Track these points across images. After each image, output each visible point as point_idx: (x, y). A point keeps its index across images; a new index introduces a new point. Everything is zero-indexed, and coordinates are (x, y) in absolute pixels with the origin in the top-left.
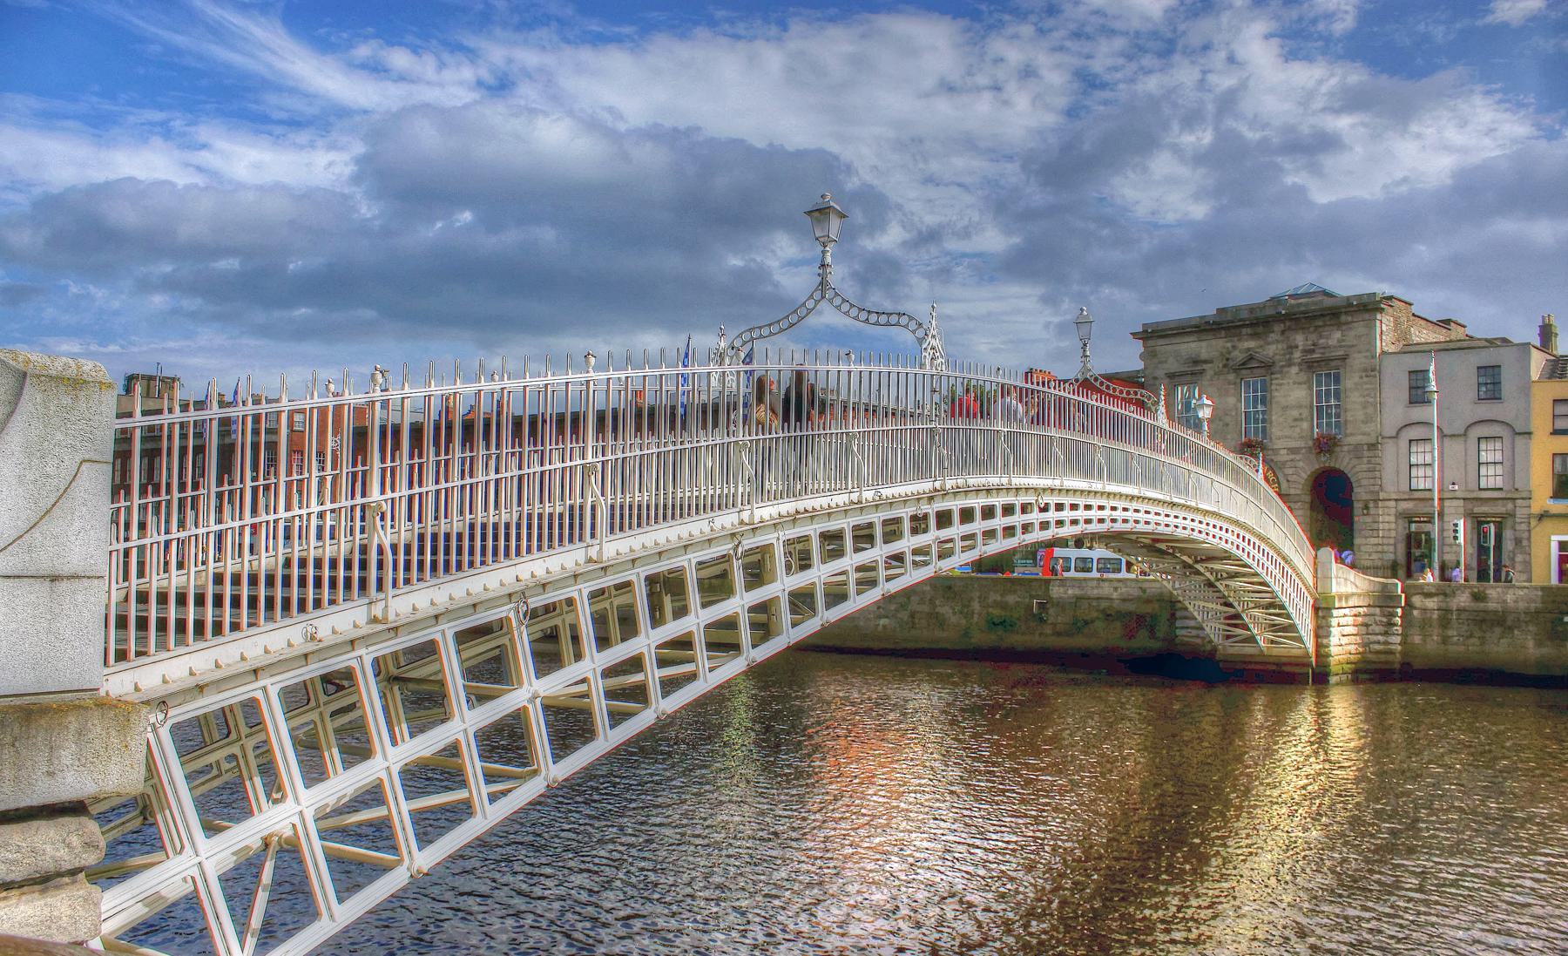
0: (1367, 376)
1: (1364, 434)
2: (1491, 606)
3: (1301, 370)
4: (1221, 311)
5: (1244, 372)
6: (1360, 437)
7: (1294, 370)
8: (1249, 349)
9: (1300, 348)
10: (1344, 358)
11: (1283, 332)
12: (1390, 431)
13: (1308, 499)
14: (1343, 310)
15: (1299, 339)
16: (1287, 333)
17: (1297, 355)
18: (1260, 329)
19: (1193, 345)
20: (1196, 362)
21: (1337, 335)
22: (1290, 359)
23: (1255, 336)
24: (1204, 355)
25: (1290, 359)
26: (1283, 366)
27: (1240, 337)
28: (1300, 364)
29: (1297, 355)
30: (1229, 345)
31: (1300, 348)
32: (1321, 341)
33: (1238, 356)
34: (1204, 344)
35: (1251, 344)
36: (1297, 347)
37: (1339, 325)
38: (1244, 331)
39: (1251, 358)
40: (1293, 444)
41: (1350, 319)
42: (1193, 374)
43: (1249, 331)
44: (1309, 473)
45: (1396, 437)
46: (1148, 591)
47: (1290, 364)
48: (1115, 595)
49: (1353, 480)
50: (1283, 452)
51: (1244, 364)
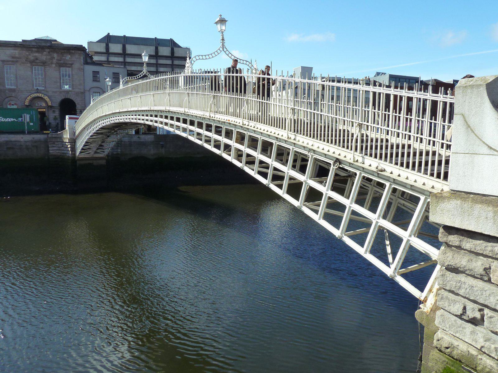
0: (80, 71)
1: (79, 89)
2: (142, 140)
3: (56, 66)
4: (23, 41)
5: (34, 64)
6: (78, 90)
7: (54, 65)
8: (36, 56)
9: (56, 59)
10: (72, 64)
11: (49, 52)
12: (87, 89)
13: (59, 108)
14: (72, 49)
15: (55, 55)
16: (50, 53)
17: (55, 61)
18: (40, 50)
19: (12, 51)
20: (13, 57)
21: (70, 56)
22: (52, 62)
23: (38, 52)
24: (17, 55)
25: (52, 62)
26: (49, 64)
27: (32, 51)
28: (55, 64)
29: (55, 61)
30: (27, 53)
31: (56, 59)
32: (63, 57)
33: (32, 58)
34: (17, 51)
35: (37, 54)
36: (54, 58)
37: (70, 53)
38: (34, 49)
39: (37, 59)
40: (55, 90)
41: (73, 52)
42: (13, 61)
43: (36, 50)
44: (60, 100)
45: (89, 91)
46: (35, 138)
47: (52, 63)
48: (22, 140)
49: (76, 103)
50: (50, 92)
51: (33, 61)
